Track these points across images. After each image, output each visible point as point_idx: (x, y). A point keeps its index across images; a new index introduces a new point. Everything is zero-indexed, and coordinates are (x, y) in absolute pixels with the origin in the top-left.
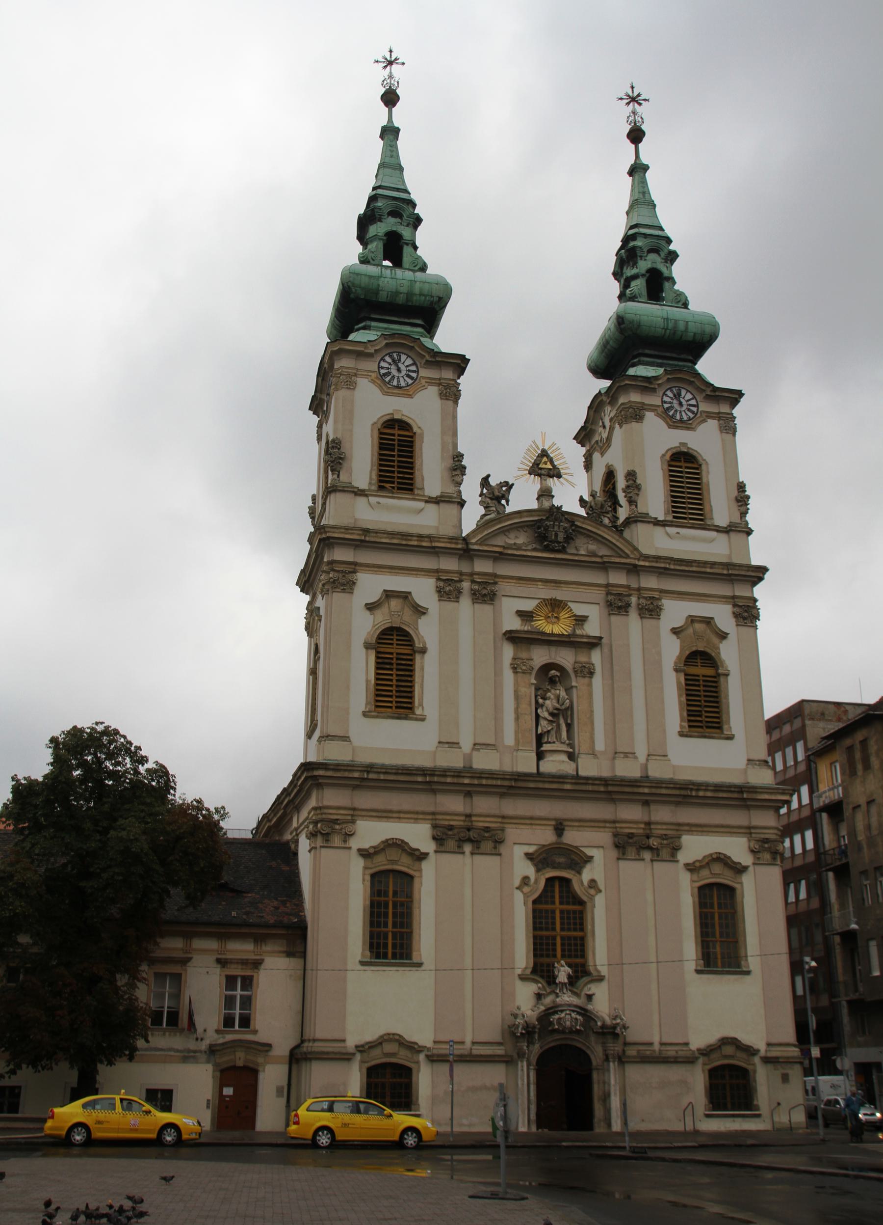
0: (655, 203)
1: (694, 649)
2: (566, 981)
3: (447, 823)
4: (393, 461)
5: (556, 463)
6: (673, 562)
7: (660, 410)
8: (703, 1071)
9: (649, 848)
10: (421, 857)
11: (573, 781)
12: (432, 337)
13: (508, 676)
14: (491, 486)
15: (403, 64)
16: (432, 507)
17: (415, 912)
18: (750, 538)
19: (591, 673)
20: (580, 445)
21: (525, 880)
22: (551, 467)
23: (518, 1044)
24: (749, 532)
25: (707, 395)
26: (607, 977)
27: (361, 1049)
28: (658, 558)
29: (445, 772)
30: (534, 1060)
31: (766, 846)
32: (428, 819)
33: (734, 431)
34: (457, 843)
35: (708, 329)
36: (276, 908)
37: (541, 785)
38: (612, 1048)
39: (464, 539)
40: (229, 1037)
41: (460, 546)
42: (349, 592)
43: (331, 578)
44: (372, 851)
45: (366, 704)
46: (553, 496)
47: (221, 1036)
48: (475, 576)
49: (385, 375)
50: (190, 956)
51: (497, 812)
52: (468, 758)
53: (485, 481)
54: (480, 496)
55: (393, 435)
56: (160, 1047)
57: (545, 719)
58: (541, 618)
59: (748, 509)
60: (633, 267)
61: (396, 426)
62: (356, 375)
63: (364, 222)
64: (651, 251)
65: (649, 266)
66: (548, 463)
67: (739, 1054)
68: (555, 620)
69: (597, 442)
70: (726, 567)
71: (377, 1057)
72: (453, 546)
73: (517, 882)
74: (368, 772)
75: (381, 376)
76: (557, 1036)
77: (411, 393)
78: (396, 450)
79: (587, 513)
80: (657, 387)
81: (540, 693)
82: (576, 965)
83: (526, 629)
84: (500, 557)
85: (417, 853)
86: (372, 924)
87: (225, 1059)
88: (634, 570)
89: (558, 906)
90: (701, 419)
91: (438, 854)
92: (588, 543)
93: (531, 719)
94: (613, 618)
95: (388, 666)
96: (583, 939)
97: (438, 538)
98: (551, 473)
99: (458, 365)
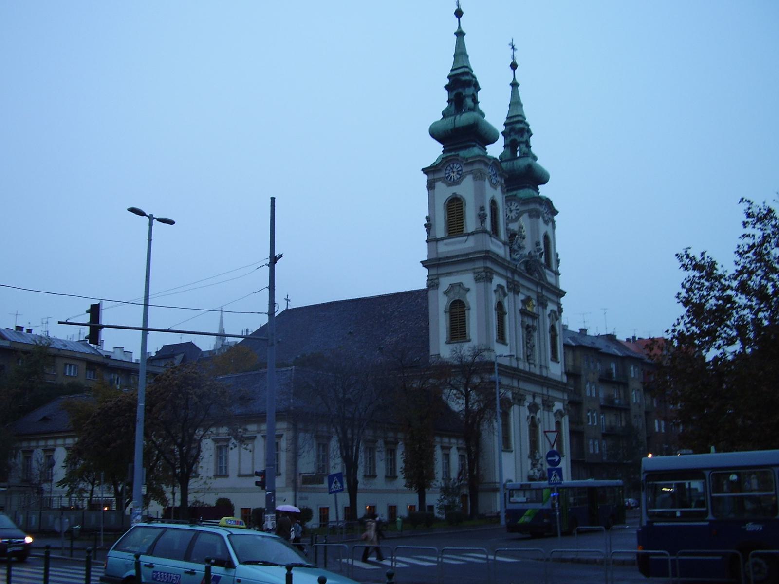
45: (447, 338)
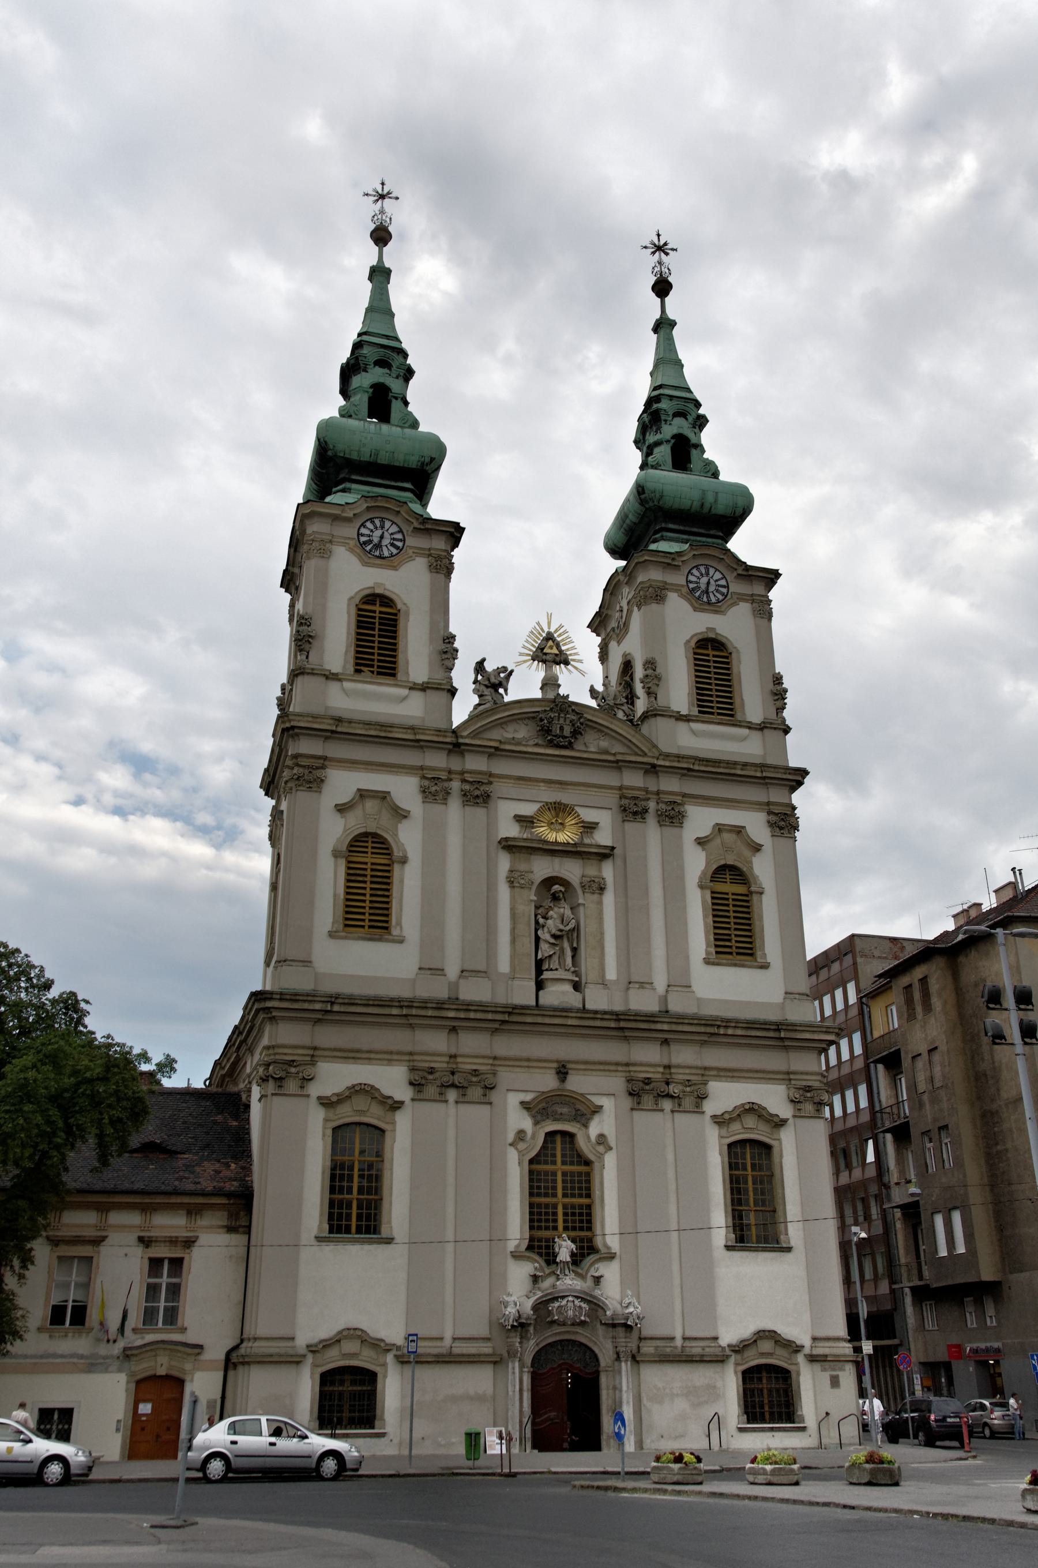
0: (683, 362)
1: (722, 862)
2: (569, 1259)
3: (427, 1065)
4: (373, 642)
5: (563, 648)
6: (697, 762)
7: (685, 590)
8: (736, 1372)
9: (668, 1096)
10: (396, 1106)
11: (579, 1015)
12: (425, 505)
13: (504, 892)
14: (486, 671)
15: (397, 198)
17: (386, 1174)
18: (787, 737)
19: (602, 889)
20: (595, 634)
21: (521, 1135)
22: (558, 652)
23: (509, 1340)
24: (787, 730)
25: (739, 575)
26: (618, 1254)
27: (313, 1349)
28: (679, 757)
29: (424, 1004)
30: (528, 1360)
31: (809, 1095)
32: (404, 1061)
33: (769, 615)
34: (438, 1089)
35: (741, 503)
36: (218, 1172)
37: (540, 1020)
38: (624, 1344)
39: (454, 732)
40: (150, 1338)
41: (448, 740)
42: (316, 791)
43: (295, 774)
44: (334, 1099)
45: (333, 923)
46: (559, 686)
47: (138, 1336)
48: (466, 775)
49: (365, 543)
50: (104, 1234)
51: (488, 1053)
52: (454, 986)
53: (480, 667)
54: (474, 683)
55: (375, 612)
56: (60, 1352)
57: (546, 941)
58: (543, 824)
59: (786, 704)
60: (656, 432)
61: (378, 602)
62: (331, 542)
63: (347, 372)
64: (676, 414)
65: (675, 431)
66: (555, 648)
67: (780, 1351)
68: (559, 827)
69: (613, 629)
70: (759, 769)
71: (333, 1360)
72: (441, 739)
73: (511, 1137)
74: (332, 1003)
75: (361, 545)
76: (557, 1329)
77: (395, 564)
78: (377, 630)
79: (599, 705)
80: (680, 564)
82: (582, 1240)
83: (525, 836)
84: (496, 752)
85: (390, 1101)
86: (332, 1190)
87: (144, 1365)
88: (652, 770)
89: (559, 1167)
90: (732, 601)
91: (416, 1103)
92: (599, 739)
93: (530, 942)
94: (628, 826)
95: (361, 879)
96: (589, 1207)
97: (424, 730)
98: (558, 659)
99: (451, 534)
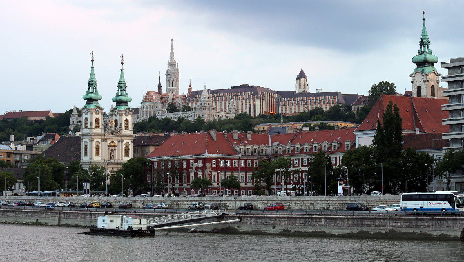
16: (101, 130)
81: (111, 153)
